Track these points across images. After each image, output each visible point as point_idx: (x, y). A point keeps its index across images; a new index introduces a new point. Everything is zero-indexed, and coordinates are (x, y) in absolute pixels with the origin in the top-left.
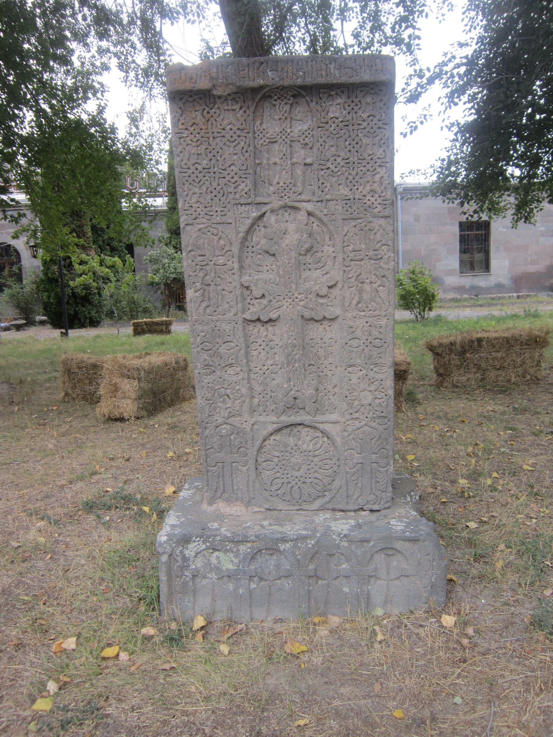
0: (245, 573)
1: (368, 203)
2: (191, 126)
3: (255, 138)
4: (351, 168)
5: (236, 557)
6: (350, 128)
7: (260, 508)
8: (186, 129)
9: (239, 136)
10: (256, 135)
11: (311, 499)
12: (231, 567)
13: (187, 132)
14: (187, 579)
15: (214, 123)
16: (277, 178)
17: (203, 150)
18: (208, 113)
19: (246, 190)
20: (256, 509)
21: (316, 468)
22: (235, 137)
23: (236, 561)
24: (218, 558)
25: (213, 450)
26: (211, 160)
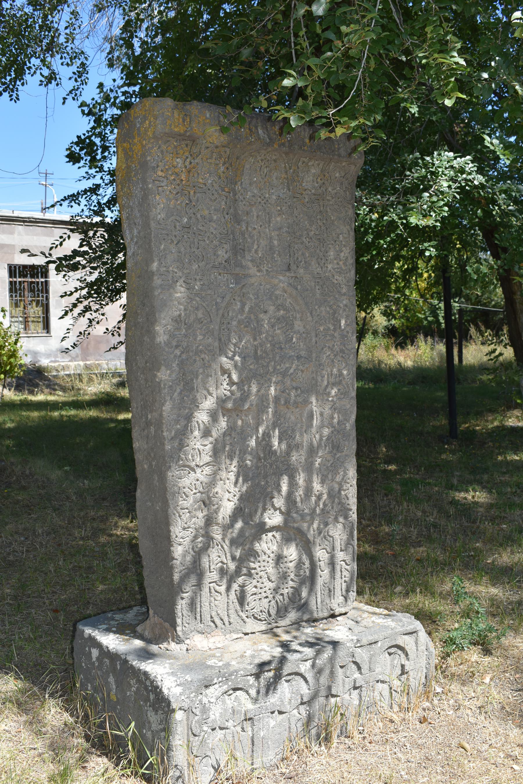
1: (336, 282)
2: (171, 175)
10: (237, 197)
15: (196, 175)
16: (255, 247)
17: (184, 204)
18: (191, 163)
19: (226, 256)
20: (235, 636)
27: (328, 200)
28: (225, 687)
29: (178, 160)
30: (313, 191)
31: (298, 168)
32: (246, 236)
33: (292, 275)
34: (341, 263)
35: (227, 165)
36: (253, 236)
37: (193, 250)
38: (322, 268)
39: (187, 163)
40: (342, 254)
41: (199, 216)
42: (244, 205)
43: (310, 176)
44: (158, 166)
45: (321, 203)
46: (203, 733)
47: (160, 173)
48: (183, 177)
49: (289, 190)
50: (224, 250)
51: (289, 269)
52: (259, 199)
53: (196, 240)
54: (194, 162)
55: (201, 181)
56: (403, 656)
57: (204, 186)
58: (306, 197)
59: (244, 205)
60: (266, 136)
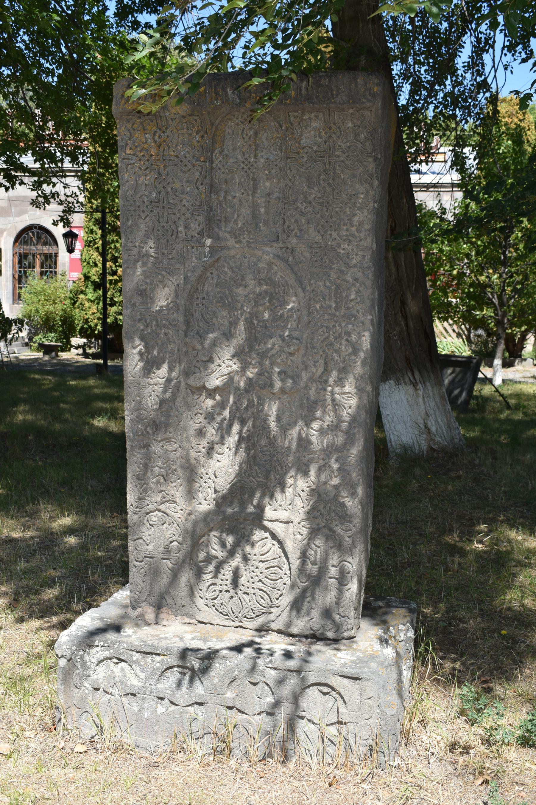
0: (151, 692)
2: (141, 151)
3: (212, 168)
4: (325, 209)
5: (143, 671)
6: (326, 161)
7: (191, 618)
8: (134, 155)
9: (194, 166)
10: (214, 165)
11: (254, 616)
12: (135, 682)
13: (134, 158)
14: (87, 691)
15: (166, 148)
17: (153, 179)
18: (160, 137)
19: (199, 229)
20: (187, 620)
21: (261, 577)
22: (190, 166)
23: (143, 676)
24: (123, 669)
25: (141, 541)
26: (160, 192)
27: (339, 156)
28: (107, 653)
29: (147, 136)
30: (315, 148)
31: (292, 124)
32: (224, 206)
33: (281, 245)
34: (354, 229)
35: (201, 133)
36: (234, 205)
37: (162, 224)
38: (322, 236)
39: (157, 138)
40: (356, 219)
41: (169, 189)
42: (223, 173)
43: (311, 131)
44: (127, 144)
45: (326, 161)
46: (83, 688)
47: (128, 151)
48: (153, 151)
49: (281, 151)
50: (197, 223)
51: (278, 239)
52: (242, 165)
53: (165, 214)
54: (164, 136)
55: (172, 153)
56: (340, 701)
57: (176, 159)
58: (305, 156)
59: (223, 173)
60: (236, 96)
